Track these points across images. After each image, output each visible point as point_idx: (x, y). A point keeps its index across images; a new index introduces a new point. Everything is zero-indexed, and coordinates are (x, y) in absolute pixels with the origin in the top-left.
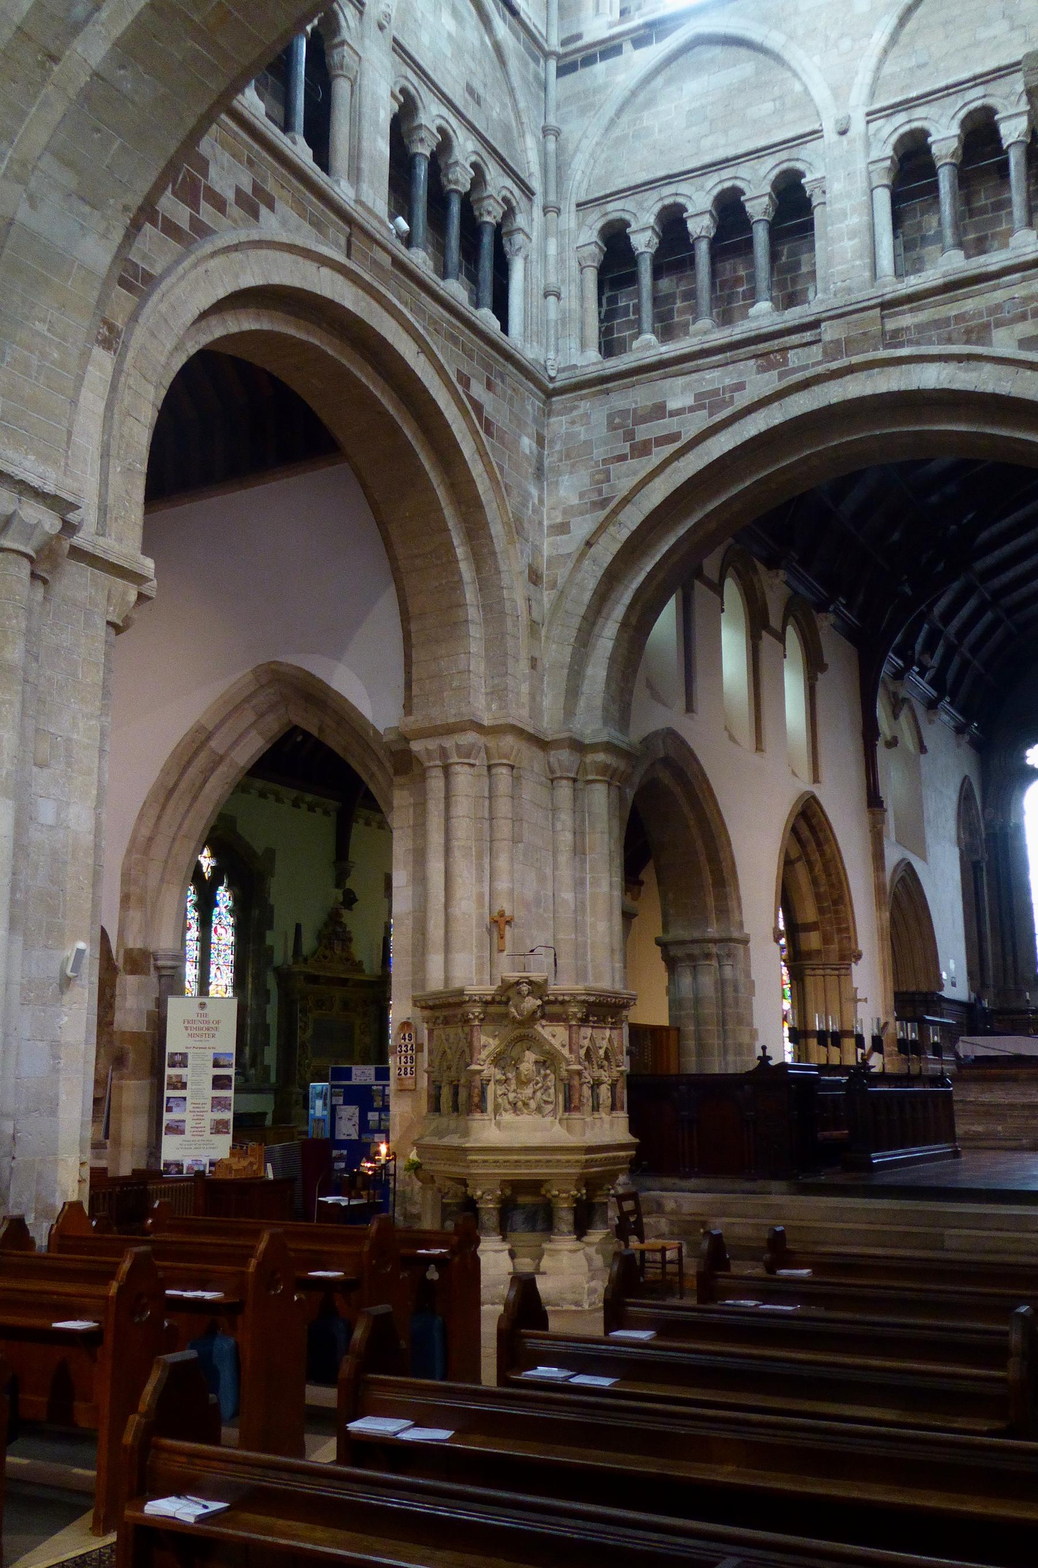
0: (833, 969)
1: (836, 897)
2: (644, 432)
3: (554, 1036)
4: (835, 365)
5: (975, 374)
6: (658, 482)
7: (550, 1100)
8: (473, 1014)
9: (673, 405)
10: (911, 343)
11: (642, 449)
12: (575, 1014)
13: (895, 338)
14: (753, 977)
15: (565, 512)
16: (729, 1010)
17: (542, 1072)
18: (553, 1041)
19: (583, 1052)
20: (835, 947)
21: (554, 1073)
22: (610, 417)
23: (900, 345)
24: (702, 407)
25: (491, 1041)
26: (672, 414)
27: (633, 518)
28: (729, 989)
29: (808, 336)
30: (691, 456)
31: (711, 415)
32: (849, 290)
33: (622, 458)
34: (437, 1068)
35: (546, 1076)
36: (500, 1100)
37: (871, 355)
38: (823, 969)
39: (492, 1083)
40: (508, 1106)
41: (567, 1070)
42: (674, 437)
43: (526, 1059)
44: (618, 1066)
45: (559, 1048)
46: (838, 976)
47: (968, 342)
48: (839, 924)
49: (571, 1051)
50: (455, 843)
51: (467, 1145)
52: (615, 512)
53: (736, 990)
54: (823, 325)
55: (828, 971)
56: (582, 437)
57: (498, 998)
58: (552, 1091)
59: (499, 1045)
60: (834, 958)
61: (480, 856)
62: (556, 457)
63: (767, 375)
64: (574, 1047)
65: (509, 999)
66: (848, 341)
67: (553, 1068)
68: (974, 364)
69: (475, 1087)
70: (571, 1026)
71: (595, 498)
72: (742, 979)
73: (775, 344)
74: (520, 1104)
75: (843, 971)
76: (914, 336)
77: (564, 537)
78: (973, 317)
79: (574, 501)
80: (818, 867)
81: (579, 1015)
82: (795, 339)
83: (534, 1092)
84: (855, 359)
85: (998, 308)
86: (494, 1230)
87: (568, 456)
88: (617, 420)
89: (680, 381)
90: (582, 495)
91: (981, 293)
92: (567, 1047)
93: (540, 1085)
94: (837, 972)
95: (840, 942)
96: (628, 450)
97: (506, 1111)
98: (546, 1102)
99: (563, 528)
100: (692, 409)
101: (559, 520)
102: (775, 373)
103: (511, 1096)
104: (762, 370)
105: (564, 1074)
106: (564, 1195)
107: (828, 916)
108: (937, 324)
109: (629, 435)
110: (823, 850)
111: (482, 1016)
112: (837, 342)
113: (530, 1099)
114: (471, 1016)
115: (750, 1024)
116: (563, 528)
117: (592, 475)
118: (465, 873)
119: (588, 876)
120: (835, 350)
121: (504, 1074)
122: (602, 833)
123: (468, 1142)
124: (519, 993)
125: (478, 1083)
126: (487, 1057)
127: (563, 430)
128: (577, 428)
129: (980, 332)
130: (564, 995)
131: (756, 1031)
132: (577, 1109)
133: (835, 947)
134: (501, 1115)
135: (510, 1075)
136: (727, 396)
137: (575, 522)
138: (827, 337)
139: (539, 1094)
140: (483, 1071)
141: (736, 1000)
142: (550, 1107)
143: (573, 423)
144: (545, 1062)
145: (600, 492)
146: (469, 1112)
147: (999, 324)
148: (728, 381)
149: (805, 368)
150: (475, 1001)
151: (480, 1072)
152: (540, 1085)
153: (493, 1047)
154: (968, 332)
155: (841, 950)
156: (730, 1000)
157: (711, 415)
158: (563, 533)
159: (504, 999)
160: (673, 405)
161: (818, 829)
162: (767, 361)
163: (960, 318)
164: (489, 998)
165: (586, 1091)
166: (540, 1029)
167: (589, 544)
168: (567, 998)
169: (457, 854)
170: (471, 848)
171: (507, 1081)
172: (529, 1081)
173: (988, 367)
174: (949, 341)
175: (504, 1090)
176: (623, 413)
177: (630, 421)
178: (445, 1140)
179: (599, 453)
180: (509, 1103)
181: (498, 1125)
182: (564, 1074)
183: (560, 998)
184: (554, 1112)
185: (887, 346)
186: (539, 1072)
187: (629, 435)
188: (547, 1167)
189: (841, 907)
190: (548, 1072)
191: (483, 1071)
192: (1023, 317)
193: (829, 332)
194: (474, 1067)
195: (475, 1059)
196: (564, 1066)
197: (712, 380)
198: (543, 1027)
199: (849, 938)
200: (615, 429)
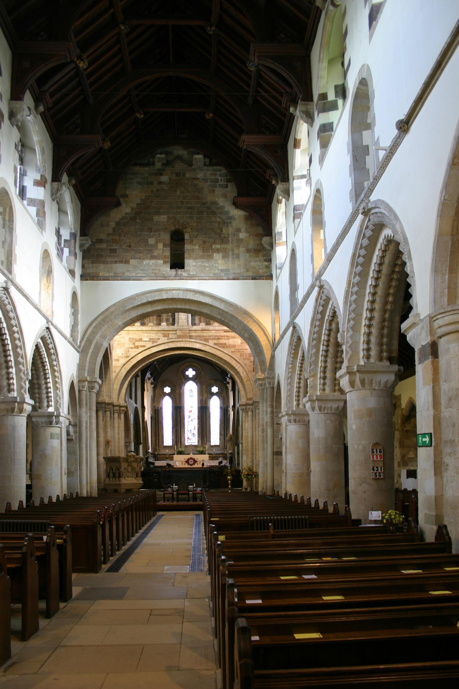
2: (137, 344)
4: (179, 340)
5: (206, 348)
6: (140, 355)
9: (144, 339)
10: (194, 339)
11: (137, 347)
13: (191, 337)
15: (118, 357)
22: (130, 339)
23: (192, 339)
24: (151, 341)
26: (144, 341)
27: (134, 361)
29: (174, 332)
30: (148, 351)
31: (152, 344)
32: (183, 326)
33: (132, 348)
37: (186, 340)
42: (144, 346)
47: (205, 341)
52: (130, 359)
54: (177, 331)
56: (123, 341)
62: (116, 344)
63: (165, 338)
66: (182, 336)
68: (205, 346)
71: (126, 355)
73: (167, 332)
76: (195, 338)
77: (118, 362)
78: (206, 337)
79: (121, 355)
82: (171, 332)
84: (183, 340)
85: (210, 336)
87: (119, 345)
88: (131, 340)
89: (146, 335)
90: (122, 354)
91: (207, 332)
96: (133, 347)
99: (118, 360)
100: (148, 341)
101: (117, 358)
102: (167, 338)
104: (164, 337)
108: (200, 336)
109: (134, 344)
112: (180, 335)
116: (118, 360)
117: (125, 350)
120: (179, 337)
127: (118, 339)
128: (121, 339)
129: (207, 340)
136: (156, 340)
137: (120, 359)
138: (178, 334)
143: (120, 338)
145: (127, 354)
147: (211, 339)
148: (156, 337)
149: (173, 339)
154: (205, 339)
157: (152, 344)
158: (117, 361)
160: (144, 339)
162: (165, 336)
163: (203, 336)
167: (124, 365)
173: (208, 347)
174: (201, 340)
176: (133, 339)
177: (134, 341)
179: (127, 346)
185: (190, 338)
187: (134, 344)
192: (215, 339)
193: (179, 333)
197: (153, 336)
200: (131, 341)
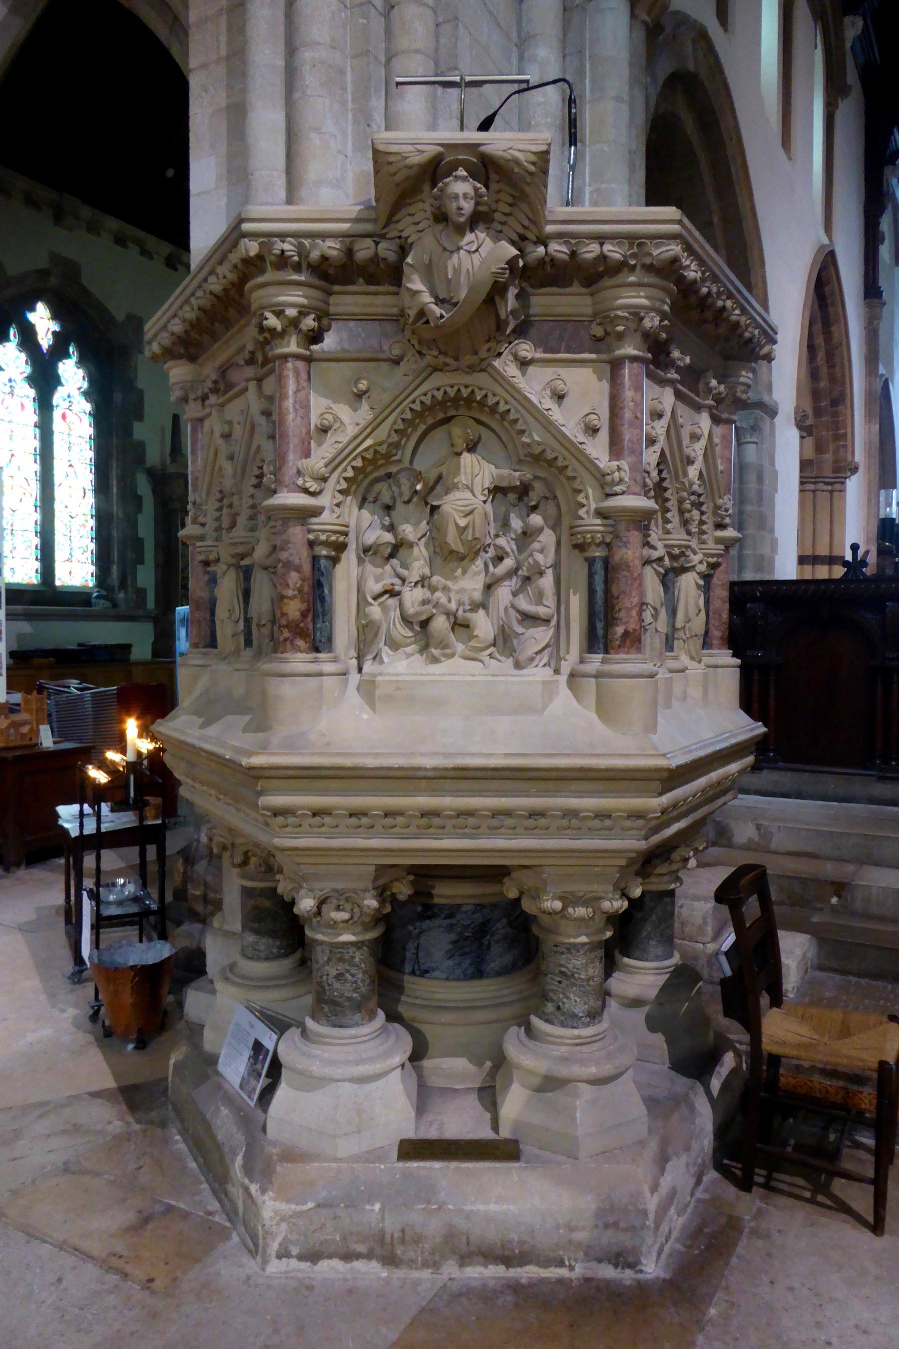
0: (827, 483)
1: (836, 394)
3: (560, 397)
7: (542, 611)
8: (279, 314)
12: (637, 315)
14: (777, 468)
16: (748, 508)
17: (516, 524)
18: (556, 414)
19: (651, 457)
20: (828, 457)
21: (555, 526)
25: (344, 412)
28: (751, 477)
34: (211, 525)
35: (527, 536)
36: (375, 611)
38: (815, 483)
39: (350, 557)
40: (402, 632)
41: (601, 514)
43: (463, 479)
44: (720, 526)
45: (572, 430)
46: (831, 492)
48: (837, 429)
49: (616, 447)
50: (306, 55)
51: (258, 760)
53: (760, 479)
55: (821, 486)
57: (364, 250)
58: (547, 582)
59: (373, 426)
60: (827, 471)
61: (362, 95)
64: (628, 435)
65: (403, 251)
67: (551, 509)
69: (289, 565)
70: (616, 365)
72: (766, 464)
74: (440, 624)
75: (837, 486)
80: (821, 355)
81: (651, 322)
83: (489, 587)
86: (358, 1007)
92: (604, 435)
93: (509, 563)
94: (829, 488)
95: (836, 451)
97: (394, 645)
98: (529, 619)
103: (413, 597)
105: (593, 524)
106: (581, 911)
107: (824, 419)
110: (830, 332)
111: (309, 322)
113: (476, 606)
114: (273, 321)
115: (772, 531)
118: (329, 126)
119: (588, 190)
121: (391, 528)
122: (618, 99)
123: (264, 748)
124: (441, 217)
125: (299, 554)
126: (333, 464)
130: (601, 239)
131: (777, 540)
132: (633, 640)
133: (828, 457)
134: (377, 657)
135: (408, 531)
139: (504, 593)
140: (317, 512)
141: (760, 493)
142: (542, 635)
144: (523, 490)
146: (277, 646)
150: (282, 261)
151: (305, 515)
152: (509, 563)
153: (351, 431)
155: (836, 461)
156: (752, 494)
159: (387, 250)
161: (829, 301)
164: (331, 248)
165: (653, 589)
166: (512, 370)
168: (615, 252)
169: (310, 79)
170: (342, 72)
171: (397, 549)
172: (474, 551)
175: (389, 580)
178: (213, 731)
180: (406, 620)
181: (368, 690)
182: (593, 524)
183: (590, 251)
184: (555, 646)
186: (505, 525)
188: (530, 831)
189: (841, 408)
190: (536, 519)
191: (317, 512)
194: (289, 498)
195: (289, 471)
196: (591, 499)
198: (524, 364)
199: (845, 446)
